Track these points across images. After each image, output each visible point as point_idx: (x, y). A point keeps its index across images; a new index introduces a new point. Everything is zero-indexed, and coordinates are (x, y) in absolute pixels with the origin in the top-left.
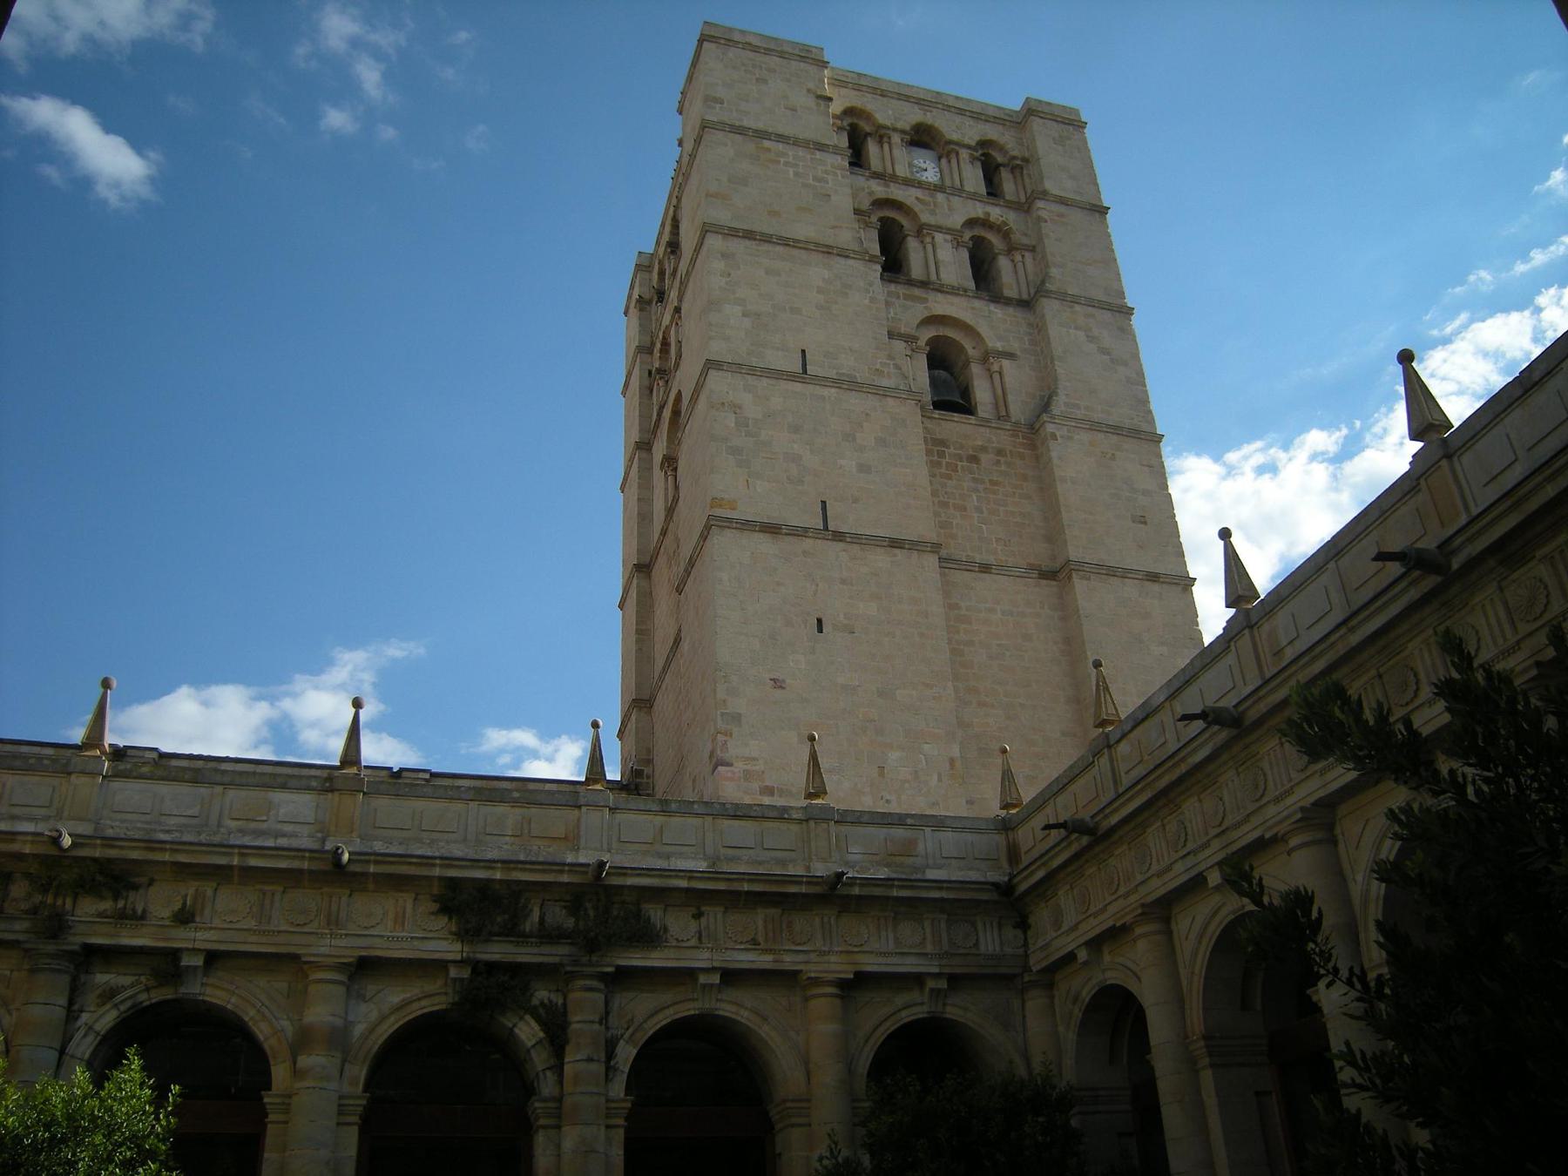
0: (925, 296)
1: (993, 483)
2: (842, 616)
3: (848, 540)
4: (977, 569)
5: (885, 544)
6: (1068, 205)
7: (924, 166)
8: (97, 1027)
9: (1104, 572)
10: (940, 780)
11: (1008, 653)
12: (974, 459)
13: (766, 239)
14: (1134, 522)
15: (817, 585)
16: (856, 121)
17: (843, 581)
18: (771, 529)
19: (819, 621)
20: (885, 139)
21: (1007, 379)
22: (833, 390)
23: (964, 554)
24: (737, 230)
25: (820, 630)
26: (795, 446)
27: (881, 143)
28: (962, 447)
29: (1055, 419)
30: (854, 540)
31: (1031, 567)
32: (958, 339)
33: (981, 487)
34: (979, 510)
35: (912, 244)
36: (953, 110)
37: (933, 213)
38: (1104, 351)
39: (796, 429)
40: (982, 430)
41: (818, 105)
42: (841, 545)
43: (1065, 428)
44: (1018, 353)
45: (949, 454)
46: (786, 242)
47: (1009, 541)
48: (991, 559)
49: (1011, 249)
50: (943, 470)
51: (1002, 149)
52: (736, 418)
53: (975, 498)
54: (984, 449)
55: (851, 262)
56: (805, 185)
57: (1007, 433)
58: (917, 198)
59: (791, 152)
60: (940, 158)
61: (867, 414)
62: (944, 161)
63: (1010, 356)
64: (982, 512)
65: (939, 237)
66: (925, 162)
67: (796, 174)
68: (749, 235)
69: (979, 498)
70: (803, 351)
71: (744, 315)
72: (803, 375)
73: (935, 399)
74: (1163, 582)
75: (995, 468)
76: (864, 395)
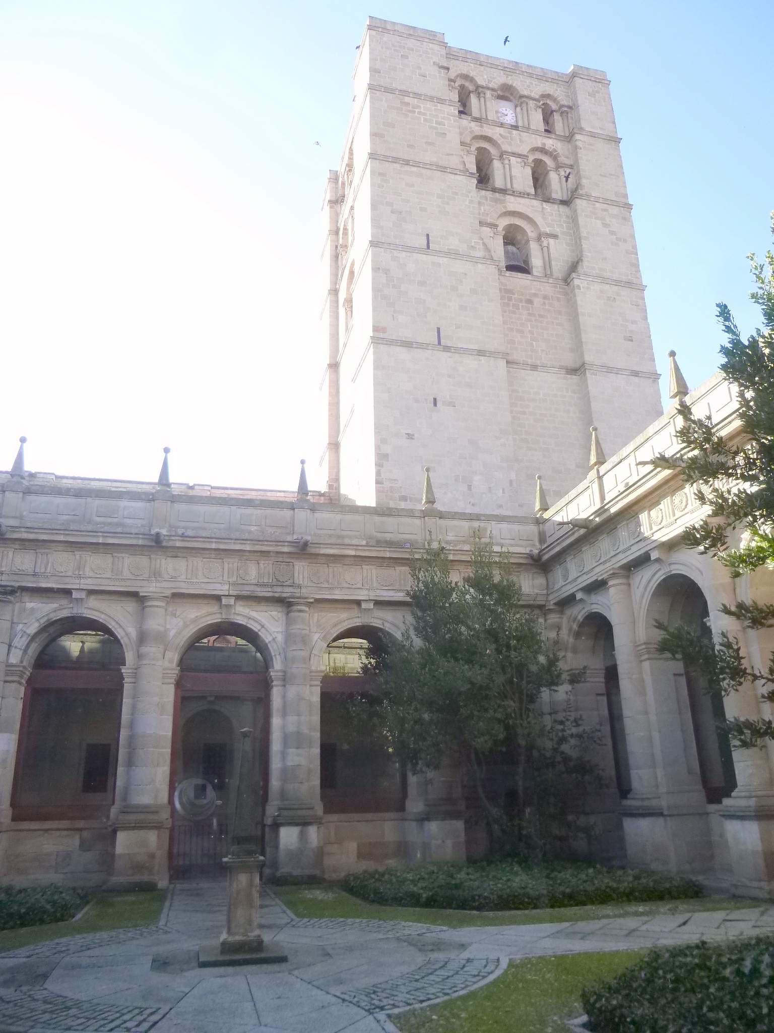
1: (540, 316)
3: (453, 351)
5: (475, 353)
8: (29, 631)
9: (605, 370)
10: (503, 492)
12: (530, 302)
18: (407, 344)
19: (435, 400)
20: (482, 95)
21: (551, 251)
22: (445, 259)
27: (479, 97)
29: (580, 276)
30: (457, 351)
31: (561, 368)
34: (531, 332)
35: (496, 164)
36: (525, 74)
37: (510, 144)
38: (612, 233)
39: (422, 283)
40: (535, 283)
41: (440, 72)
42: (449, 354)
43: (586, 282)
49: (558, 167)
51: (555, 100)
54: (535, 295)
55: (458, 177)
56: (431, 127)
58: (500, 134)
60: (516, 106)
61: (466, 274)
62: (518, 109)
63: (555, 236)
64: (533, 334)
65: (513, 159)
66: (506, 110)
67: (425, 120)
71: (392, 212)
73: (509, 264)
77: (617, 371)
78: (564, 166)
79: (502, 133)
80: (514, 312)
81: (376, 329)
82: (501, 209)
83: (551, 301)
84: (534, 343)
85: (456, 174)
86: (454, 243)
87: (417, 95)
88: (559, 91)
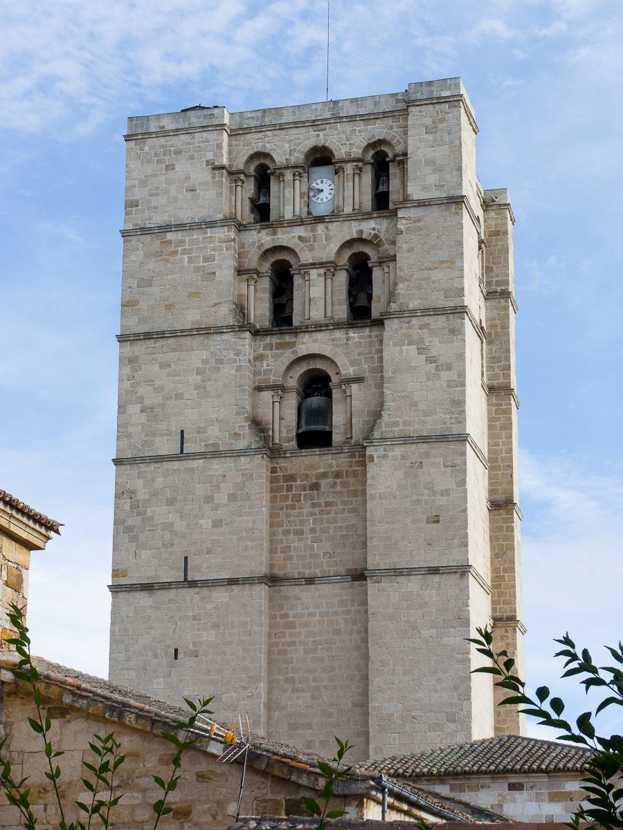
0: (293, 340)
1: (328, 504)
2: (191, 645)
4: (304, 583)
5: (225, 583)
6: (426, 205)
7: (320, 187)
9: (392, 574)
11: (320, 647)
12: (315, 486)
13: (162, 335)
14: (428, 522)
15: (176, 624)
16: (262, 161)
17: (194, 618)
18: (148, 587)
19: (176, 650)
22: (201, 461)
23: (296, 571)
24: (139, 335)
25: (176, 657)
26: (170, 516)
28: (307, 476)
30: (204, 585)
32: (324, 369)
33: (317, 510)
34: (313, 531)
37: (312, 249)
38: (431, 360)
39: (171, 502)
40: (325, 457)
41: (214, 176)
42: (196, 590)
43: (382, 448)
44: (366, 375)
45: (296, 487)
46: (175, 334)
47: (334, 552)
48: (318, 572)
50: (289, 502)
52: (131, 502)
53: (311, 521)
54: (324, 475)
55: (225, 337)
56: (197, 269)
57: (346, 455)
58: (300, 238)
59: (188, 237)
61: (224, 476)
64: (315, 532)
66: (322, 182)
67: (191, 260)
68: (148, 336)
69: (314, 520)
70: (182, 431)
72: (182, 455)
74: (443, 573)
75: (332, 490)
76: (223, 459)
77: (409, 572)
78: (385, 260)
79: (303, 234)
80: (293, 507)
81: (116, 573)
82: (288, 356)
83: (345, 479)
84: (315, 544)
85: (223, 332)
86: (216, 435)
87: (181, 227)
88: (395, 129)
